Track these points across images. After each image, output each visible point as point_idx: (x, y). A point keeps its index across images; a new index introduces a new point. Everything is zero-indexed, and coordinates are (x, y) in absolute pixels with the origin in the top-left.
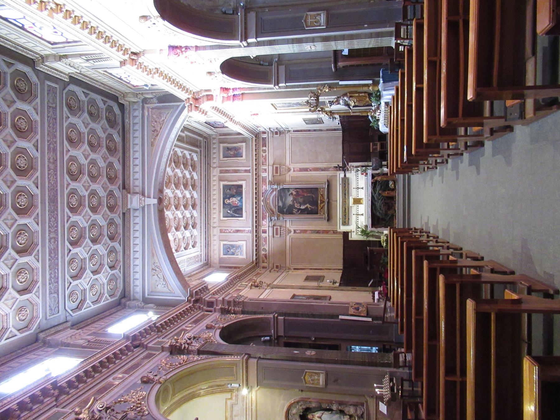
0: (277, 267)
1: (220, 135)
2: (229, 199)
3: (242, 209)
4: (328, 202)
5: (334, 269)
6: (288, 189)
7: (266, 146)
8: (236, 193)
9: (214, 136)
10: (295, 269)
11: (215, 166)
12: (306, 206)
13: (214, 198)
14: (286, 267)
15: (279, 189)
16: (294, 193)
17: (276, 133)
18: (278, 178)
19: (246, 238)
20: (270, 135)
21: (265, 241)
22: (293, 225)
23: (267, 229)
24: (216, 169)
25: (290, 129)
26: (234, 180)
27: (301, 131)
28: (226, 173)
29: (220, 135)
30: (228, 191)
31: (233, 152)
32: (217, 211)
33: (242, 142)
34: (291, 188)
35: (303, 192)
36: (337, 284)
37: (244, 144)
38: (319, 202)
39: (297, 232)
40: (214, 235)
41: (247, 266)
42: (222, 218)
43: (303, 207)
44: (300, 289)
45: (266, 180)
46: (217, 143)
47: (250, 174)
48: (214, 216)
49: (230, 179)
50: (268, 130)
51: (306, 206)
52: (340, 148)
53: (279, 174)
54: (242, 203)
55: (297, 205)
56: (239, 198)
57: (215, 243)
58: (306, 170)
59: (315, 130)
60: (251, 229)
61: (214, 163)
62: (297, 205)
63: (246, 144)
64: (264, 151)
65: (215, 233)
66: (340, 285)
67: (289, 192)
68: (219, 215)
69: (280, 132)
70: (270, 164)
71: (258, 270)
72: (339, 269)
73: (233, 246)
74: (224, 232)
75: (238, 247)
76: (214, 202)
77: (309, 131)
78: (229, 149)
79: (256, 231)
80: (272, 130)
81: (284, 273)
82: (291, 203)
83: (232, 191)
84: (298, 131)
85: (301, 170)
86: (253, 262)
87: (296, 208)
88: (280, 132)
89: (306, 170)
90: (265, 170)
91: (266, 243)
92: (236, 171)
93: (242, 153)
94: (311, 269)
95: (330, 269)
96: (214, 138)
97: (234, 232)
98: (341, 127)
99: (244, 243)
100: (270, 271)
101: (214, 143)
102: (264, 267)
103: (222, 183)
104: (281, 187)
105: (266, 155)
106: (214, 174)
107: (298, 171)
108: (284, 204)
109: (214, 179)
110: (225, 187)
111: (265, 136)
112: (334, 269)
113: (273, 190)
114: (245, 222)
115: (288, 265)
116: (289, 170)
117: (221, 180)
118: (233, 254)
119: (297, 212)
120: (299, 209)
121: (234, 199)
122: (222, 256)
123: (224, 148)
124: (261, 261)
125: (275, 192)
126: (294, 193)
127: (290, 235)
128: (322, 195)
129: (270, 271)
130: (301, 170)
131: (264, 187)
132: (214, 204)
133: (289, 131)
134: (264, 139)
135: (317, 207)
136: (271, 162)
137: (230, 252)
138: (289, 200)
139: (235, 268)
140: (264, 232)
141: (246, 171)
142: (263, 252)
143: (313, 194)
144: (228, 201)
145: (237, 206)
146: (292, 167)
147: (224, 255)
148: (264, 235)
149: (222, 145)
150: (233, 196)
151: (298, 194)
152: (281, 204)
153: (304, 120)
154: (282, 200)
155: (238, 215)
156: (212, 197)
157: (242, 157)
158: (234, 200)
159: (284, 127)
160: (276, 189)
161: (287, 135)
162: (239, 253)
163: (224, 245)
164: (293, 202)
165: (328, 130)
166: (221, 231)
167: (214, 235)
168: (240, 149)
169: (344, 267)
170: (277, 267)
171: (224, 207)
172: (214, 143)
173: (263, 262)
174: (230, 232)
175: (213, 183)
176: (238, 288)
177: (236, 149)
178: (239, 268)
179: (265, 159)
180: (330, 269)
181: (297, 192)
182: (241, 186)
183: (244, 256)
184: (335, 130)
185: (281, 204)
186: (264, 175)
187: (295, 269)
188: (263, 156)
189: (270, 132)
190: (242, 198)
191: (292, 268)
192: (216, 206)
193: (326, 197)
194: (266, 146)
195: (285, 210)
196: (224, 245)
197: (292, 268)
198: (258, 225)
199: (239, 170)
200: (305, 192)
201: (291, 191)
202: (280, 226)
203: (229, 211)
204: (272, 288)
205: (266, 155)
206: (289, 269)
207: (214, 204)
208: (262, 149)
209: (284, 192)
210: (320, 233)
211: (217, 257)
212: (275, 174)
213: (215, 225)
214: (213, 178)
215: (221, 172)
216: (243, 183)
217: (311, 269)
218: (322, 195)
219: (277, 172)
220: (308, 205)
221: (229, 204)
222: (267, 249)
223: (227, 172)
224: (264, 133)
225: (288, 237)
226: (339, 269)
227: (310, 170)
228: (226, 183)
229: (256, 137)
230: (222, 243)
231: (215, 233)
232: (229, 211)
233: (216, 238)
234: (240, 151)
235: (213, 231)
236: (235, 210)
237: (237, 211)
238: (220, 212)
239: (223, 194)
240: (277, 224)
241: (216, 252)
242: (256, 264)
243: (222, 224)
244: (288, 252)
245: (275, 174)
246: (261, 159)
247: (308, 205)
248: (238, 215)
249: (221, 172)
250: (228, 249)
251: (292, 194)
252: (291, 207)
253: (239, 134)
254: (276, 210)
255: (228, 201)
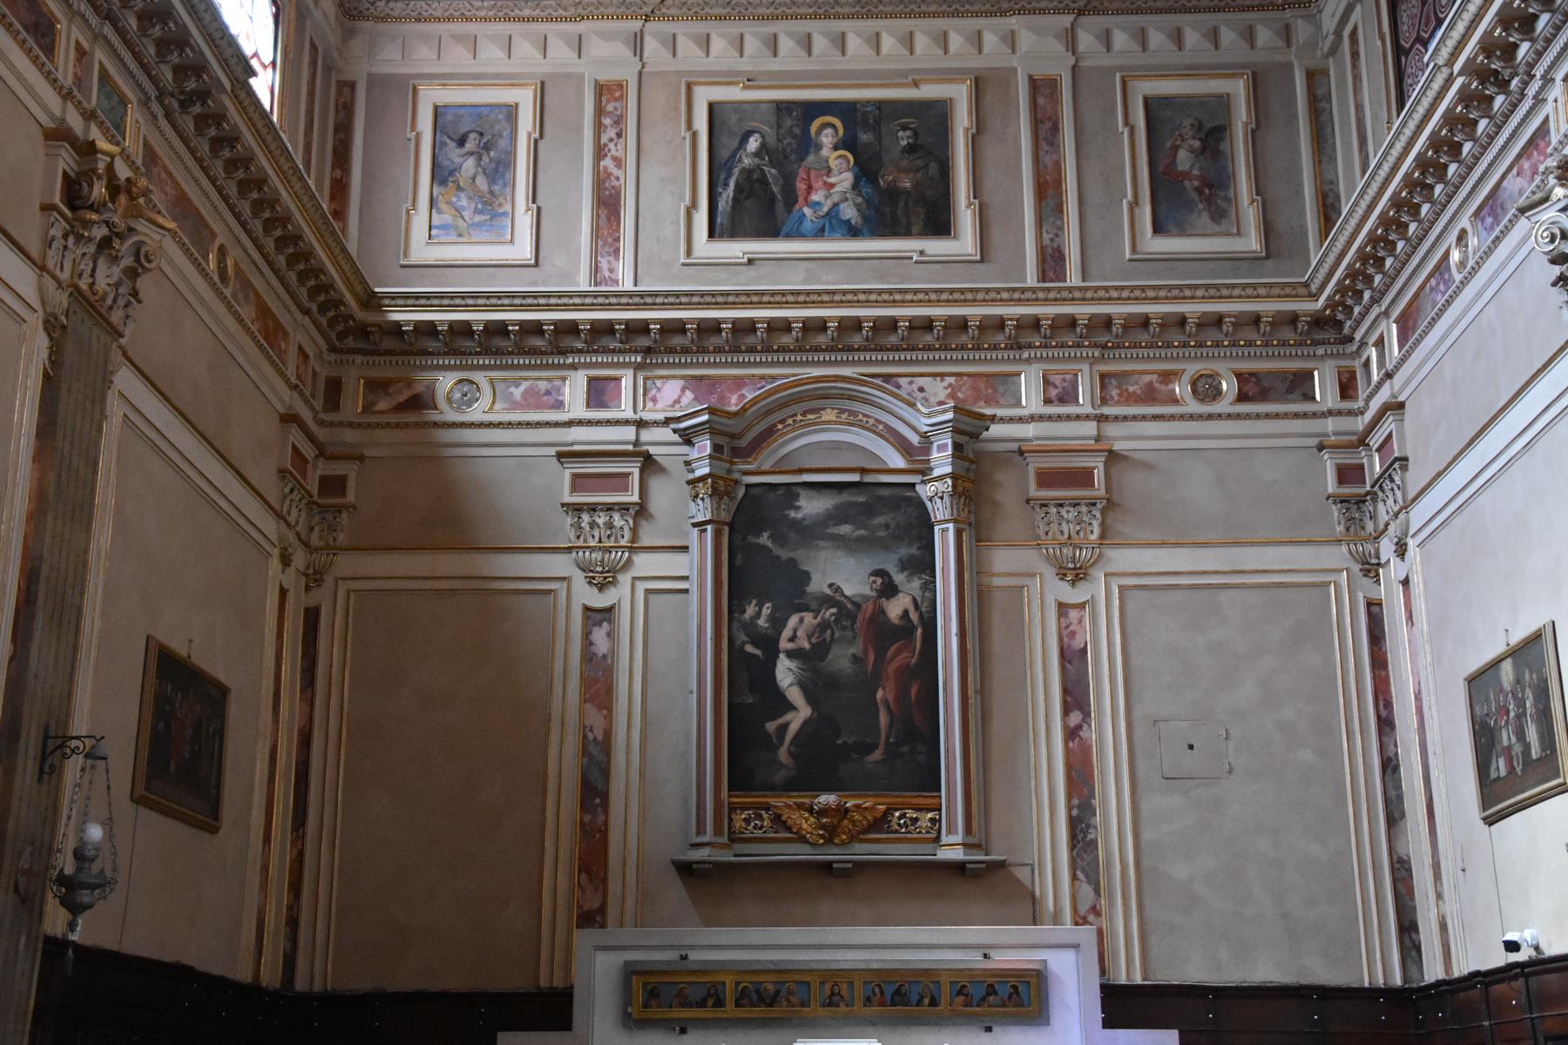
0: (333, 485)
1: (1311, 75)
2: (847, 143)
3: (771, 230)
4: (827, 867)
5: (293, 922)
6: (923, 565)
7: (1242, 397)
8: (893, 193)
9: (1302, 30)
10: (312, 617)
11: (1086, 40)
12: (795, 695)
13: (853, 42)
14: (333, 549)
15: (926, 491)
16: (895, 609)
17: (1348, 474)
18: (1009, 490)
19: (555, 259)
20: (1330, 424)
21: (533, 400)
22: (654, 608)
23: (625, 410)
24: (1059, 48)
25: (1394, 570)
26: (991, 174)
27: (1379, 662)
28: (1036, 122)
29: (1315, 77)
30: (904, 139)
31: (1188, 167)
32: (754, 57)
33: (1268, 230)
34: (930, 586)
35: (906, 676)
36: (55, 919)
37: (1252, 242)
38: (828, 799)
39: (599, 635)
40: (579, 45)
41: (356, 278)
42: (704, 96)
43: (786, 673)
44: (30, 576)
45: (989, 402)
46: (1258, 57)
47: (1031, 280)
48: (717, 44)
49: (991, 152)
50: (1383, 396)
51: (795, 695)
52: (1265, 971)
53: (1034, 491)
54: (819, 233)
55: (799, 628)
56: (849, 212)
57: (526, 50)
58: (1075, 697)
59: (1390, 766)
60: (628, 286)
61: (1106, 38)
62: (799, 628)
63: (1252, 259)
64: (1206, 389)
65: (598, 48)
66: (54, 947)
67: (907, 565)
68: (726, 78)
69: (1360, 501)
70: (1111, 430)
71: (302, 333)
72: (290, 963)
73: (500, 170)
74: (600, 112)
75: (492, 208)
76: (820, 43)
77: (1386, 724)
78: (1213, 137)
79: (607, 328)
80: (1389, 425)
81: (269, 525)
82: (818, 585)
83: (903, 171)
84: (1377, 636)
85: (1073, 660)
86: (372, 301)
87: (778, 622)
88: (1360, 501)
89: (1075, 697)
90: (1068, 397)
91: (515, 406)
92: (1048, 189)
93: (1183, 232)
94: (305, 741)
95: (296, 888)
96: (1287, 33)
97: (600, 180)
98: (1433, 971)
99: (523, 250)
100: (289, 419)
101: (1249, 35)
102: (334, 388)
103: (960, 95)
104: (940, 510)
105: (1175, 401)
106: (1026, 40)
107: (1065, 635)
108: (810, 532)
109: (990, 40)
110: (935, 116)
111: (1324, 389)
112: (293, 922)
113: (917, 454)
114: (675, 251)
115: (346, 564)
116: (1077, 574)
117: (979, 86)
118: (441, 175)
119: (749, 627)
120: (770, 645)
121: (843, 180)
122: (431, 95)
123: (1223, 103)
124: (383, 369)
125: (898, 461)
126: (895, 609)
127: (579, 578)
128: (880, 823)
129: (289, 419)
130: (1073, 660)
131: (938, 390)
132: (807, 44)
133: (1371, 568)
134: (1299, 384)
135: (791, 786)
136: (1123, 438)
137: (453, 154)
138: (842, 573)
139: (340, 189)
140: (599, 393)
141: (1051, 262)
142: (446, 382)
143: (892, 753)
144: (827, 139)
145: (791, 199)
146: (1096, 587)
147: (438, 112)
148: (574, 389)
149: (1238, 89)
150: (866, 170)
151: (884, 634)
152: (811, 507)
153: (1537, 637)
154: (839, 515)
155: (724, 204)
156: (856, 33)
157: (1158, 229)
158: (834, 180)
159: (1418, 515)
160: (925, 471)
161: (1337, 556)
162: (447, 218)
163: (511, 111)
164: (827, 601)
165: (1401, 870)
166: (604, 91)
167: (579, 45)
168: (1218, 215)
169: (309, 997)
170: (333, 485)
171: (782, 107)
172: (1249, 35)
173: (377, 386)
174: (600, 152)
175: (958, 33)
176: (69, 34)
177: (1212, 195)
178: (340, 214)
179: (1150, 396)
180: (296, 888)
181: (904, 630)
182: (940, 225)
183: (421, 251)
184: (1408, 928)
185: (811, 507)
186: (1029, 391)
187: (312, 617)
188: (1167, 377)
189: (1361, 423)
190: (853, 232)
191: (322, 596)
192: (790, 55)
193: (864, 851)
194: (1242, 397)
195: (765, 539)
196: (511, 111)
197: (322, 596)
198: (653, 343)
199: (1059, 209)
200: (902, 692)
201: (910, 586)
202: (641, 511)
203: (753, 144)
204: (50, 324)
205: (1175, 401)
206: (314, 578)
207: (807, 44)
208: (1220, 367)
209: (899, 535)
210: (584, 808)
211: (423, 59)
212: (1034, 464)
213: (651, 45)
214: (992, 32)
215: (1042, 88)
216: (964, 242)
217: (305, 741)
218: (880, 823)
219: (1047, 479)
220: (804, 711)
221: (806, 145)
222: (476, 413)
223: (1045, 129)
224: (1347, 388)
225: (561, 565)
226: (290, 963)
227: (1071, 733)
228: (962, 121)
229: (1318, 322)
230: (525, 99)
231: (598, 48)
232: (753, 144)
233: (560, 53)
234: (1203, 219)
235: (605, 36)
236: (763, 181)
237: (754, 197)
238: (750, 81)
239: (879, 105)
240: (656, 485)
241: (458, 59)
242: (363, 331)
243: (657, 99)
244: (449, 564)
245: (1034, 464)
246: (1143, 367)
247: (804, 711)
248: (724, 204)
249: (1042, 88)
250: (475, 141)
251: (889, 590)
252: (792, 590)
253: (1328, 211)
254: (757, 473)
255: (827, 139)
